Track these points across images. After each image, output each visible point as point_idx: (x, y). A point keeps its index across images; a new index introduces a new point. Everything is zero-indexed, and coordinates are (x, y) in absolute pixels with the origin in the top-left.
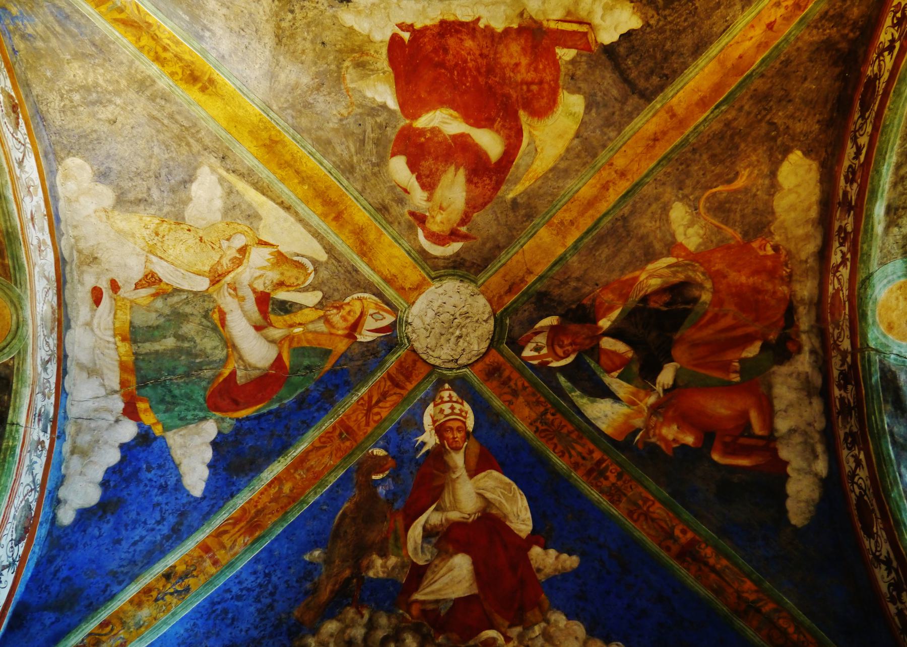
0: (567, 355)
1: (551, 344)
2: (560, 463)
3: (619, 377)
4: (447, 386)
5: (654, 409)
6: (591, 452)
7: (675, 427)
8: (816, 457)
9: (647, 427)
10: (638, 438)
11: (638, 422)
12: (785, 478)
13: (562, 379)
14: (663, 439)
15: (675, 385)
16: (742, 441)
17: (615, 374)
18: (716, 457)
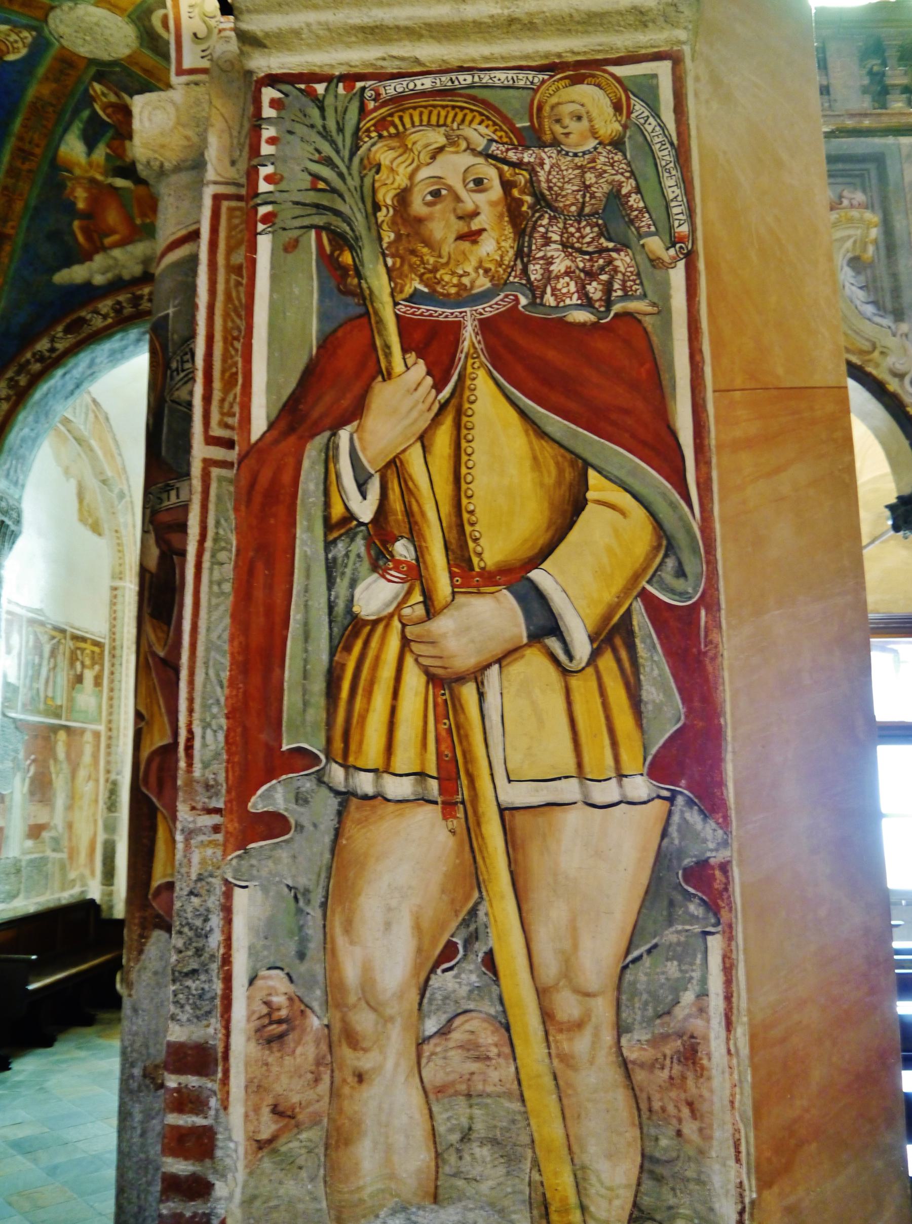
0: (108, 116)
1: (112, 105)
2: (17, 125)
3: (107, 155)
4: (34, 33)
5: (93, 181)
6: (38, 146)
7: (85, 195)
8: (103, 274)
9: (77, 179)
10: (65, 174)
11: (78, 172)
12: (81, 262)
13: (86, 114)
14: (73, 190)
15: (116, 189)
16: (95, 236)
17: (108, 151)
18: (76, 224)
